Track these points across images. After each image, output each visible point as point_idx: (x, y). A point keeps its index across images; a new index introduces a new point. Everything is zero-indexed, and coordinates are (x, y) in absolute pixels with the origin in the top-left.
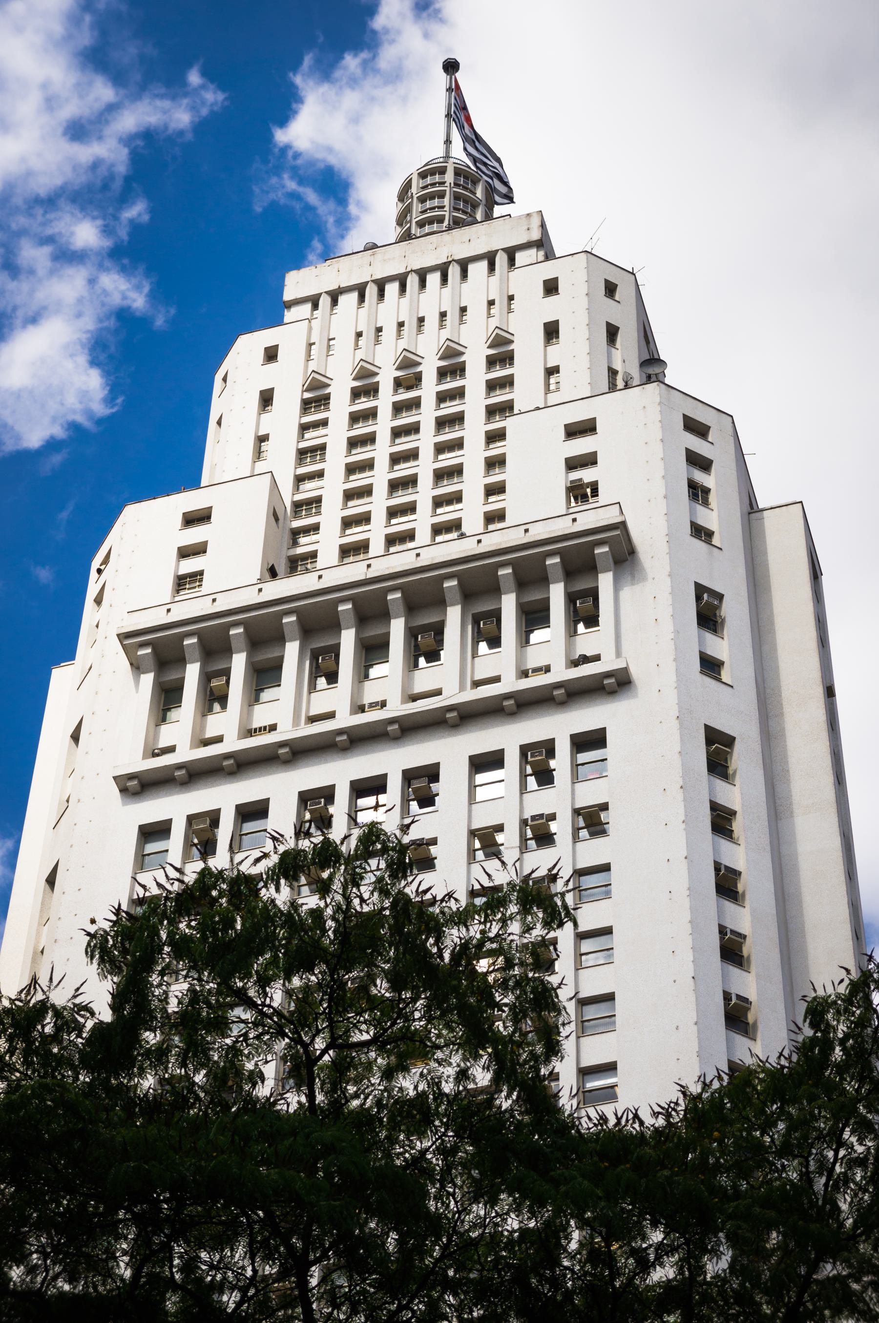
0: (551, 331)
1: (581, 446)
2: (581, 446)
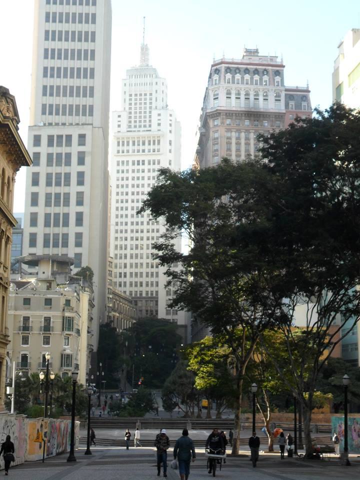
0: (156, 91)
1: (159, 118)
2: (159, 118)
